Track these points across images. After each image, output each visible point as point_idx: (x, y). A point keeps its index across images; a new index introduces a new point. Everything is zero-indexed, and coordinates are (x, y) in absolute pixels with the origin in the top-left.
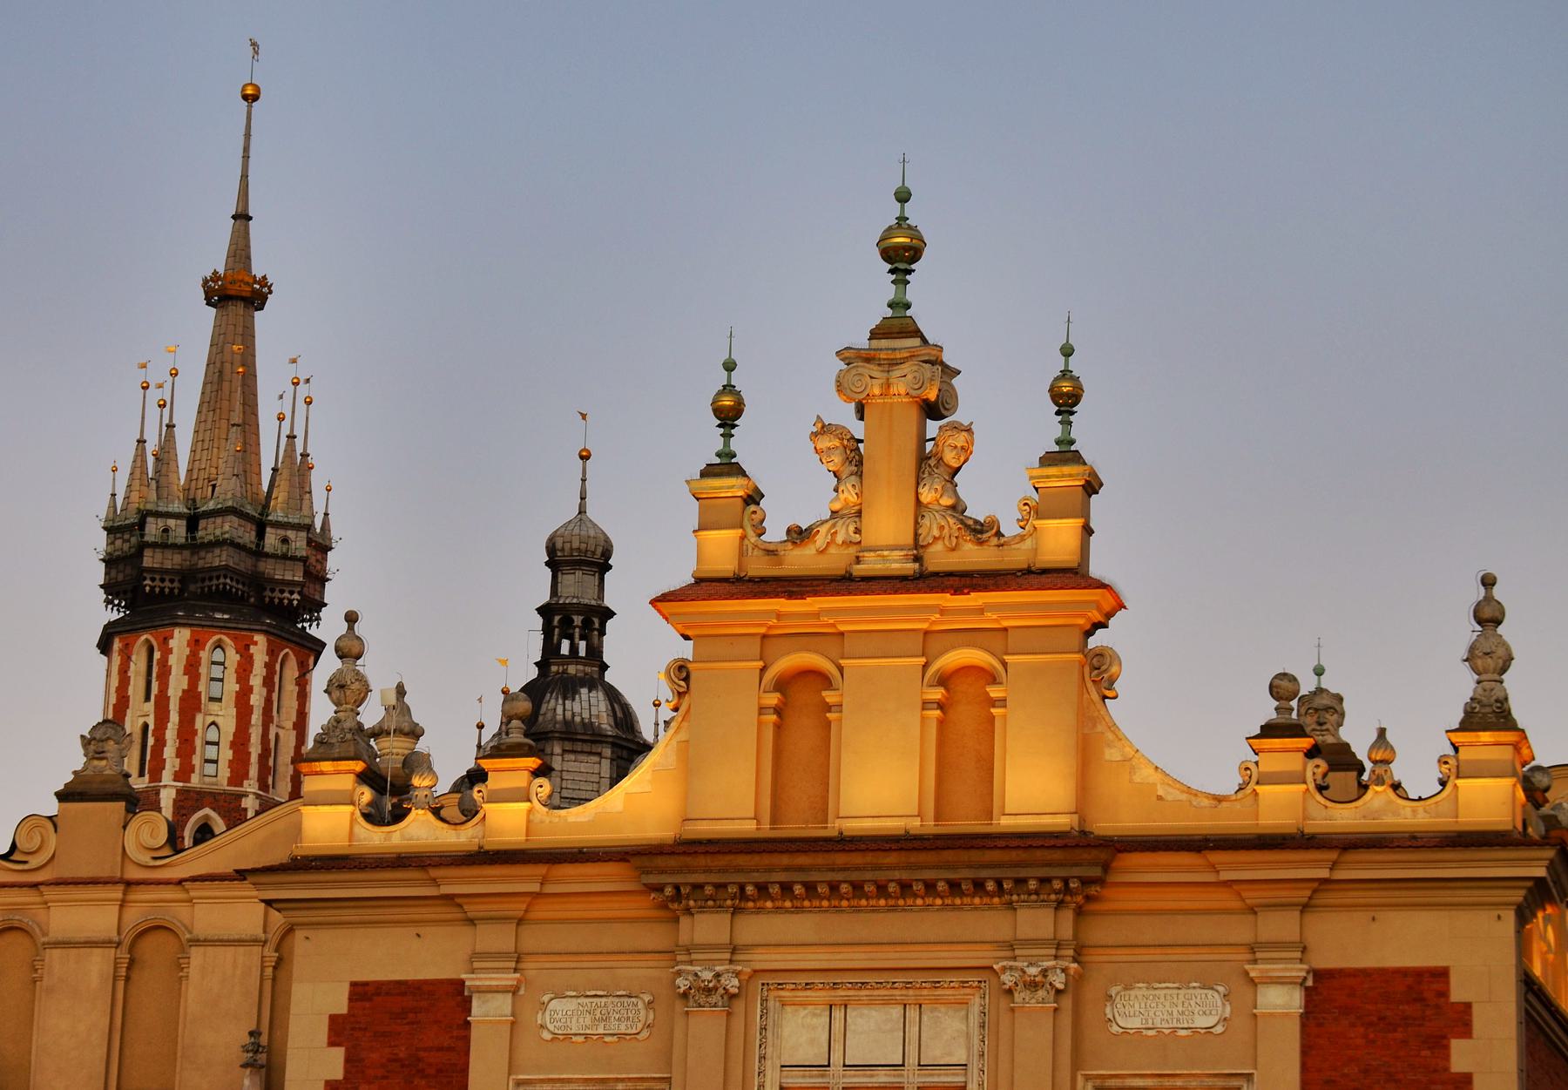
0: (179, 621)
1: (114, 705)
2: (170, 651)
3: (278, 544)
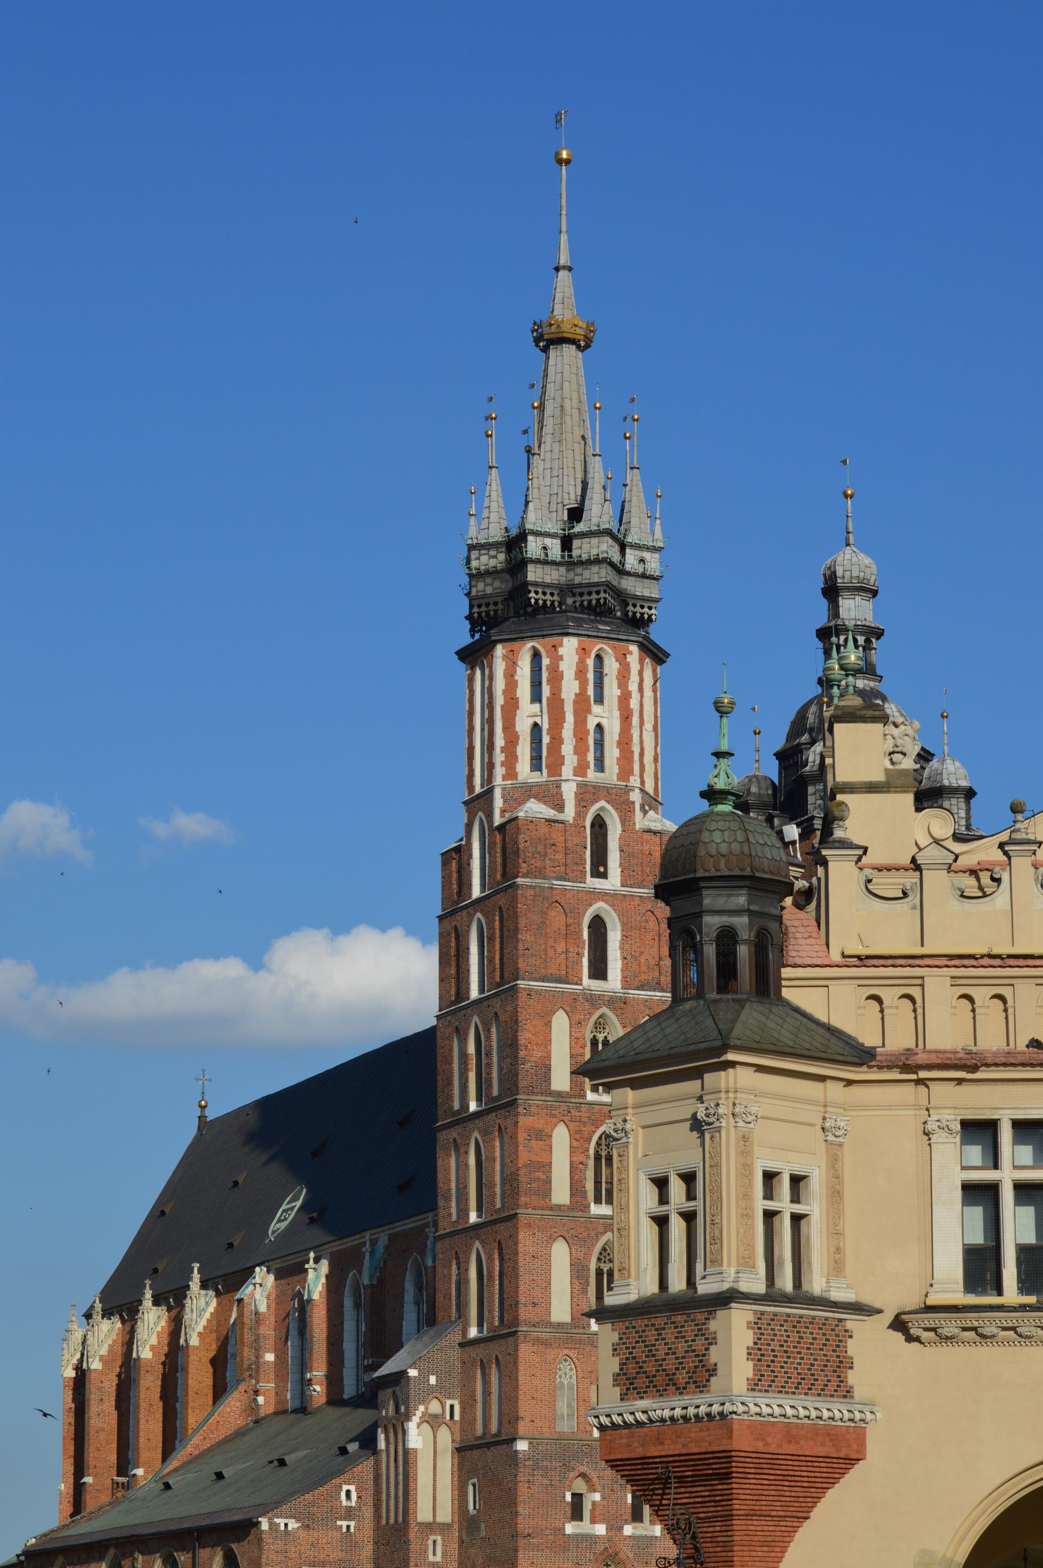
0: (570, 631)
1: (502, 706)
2: (561, 658)
3: (636, 562)
